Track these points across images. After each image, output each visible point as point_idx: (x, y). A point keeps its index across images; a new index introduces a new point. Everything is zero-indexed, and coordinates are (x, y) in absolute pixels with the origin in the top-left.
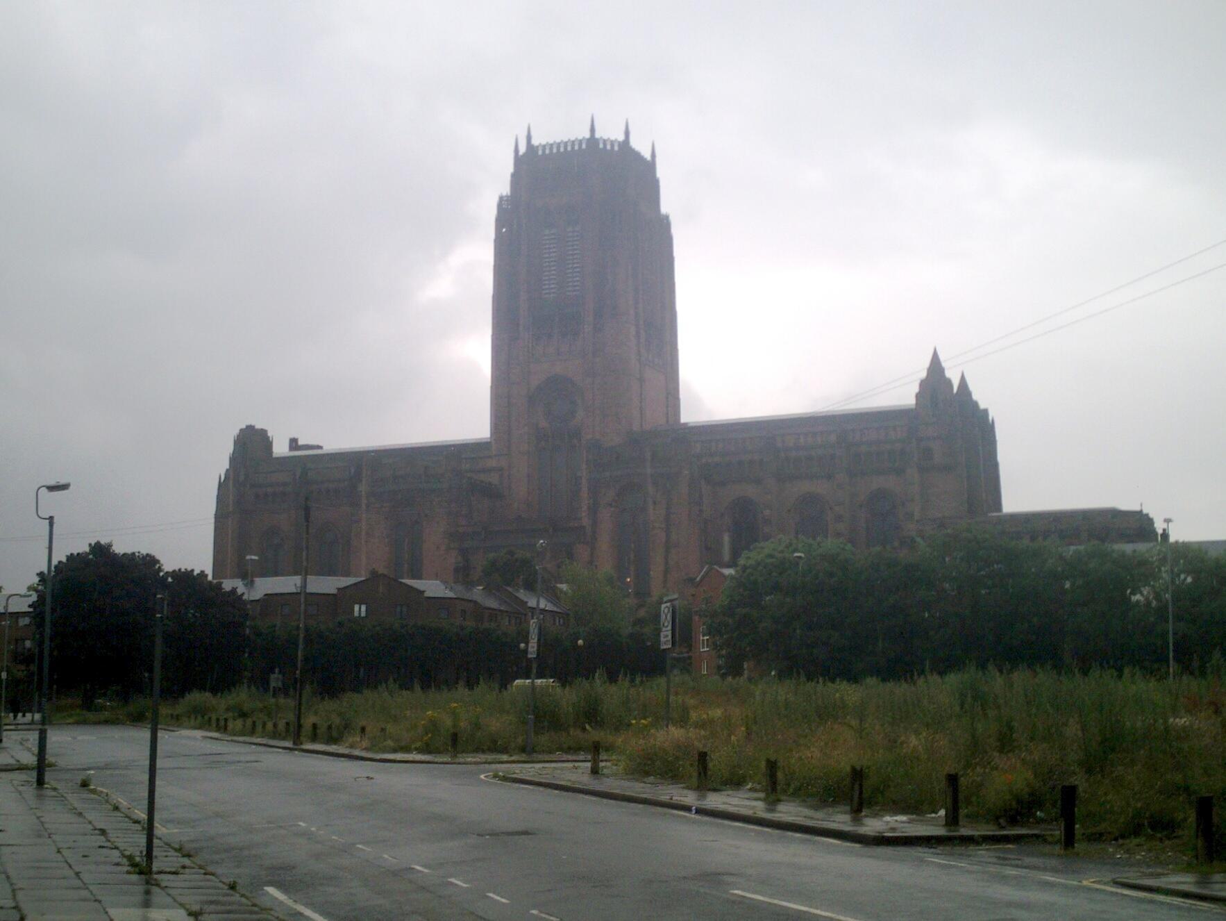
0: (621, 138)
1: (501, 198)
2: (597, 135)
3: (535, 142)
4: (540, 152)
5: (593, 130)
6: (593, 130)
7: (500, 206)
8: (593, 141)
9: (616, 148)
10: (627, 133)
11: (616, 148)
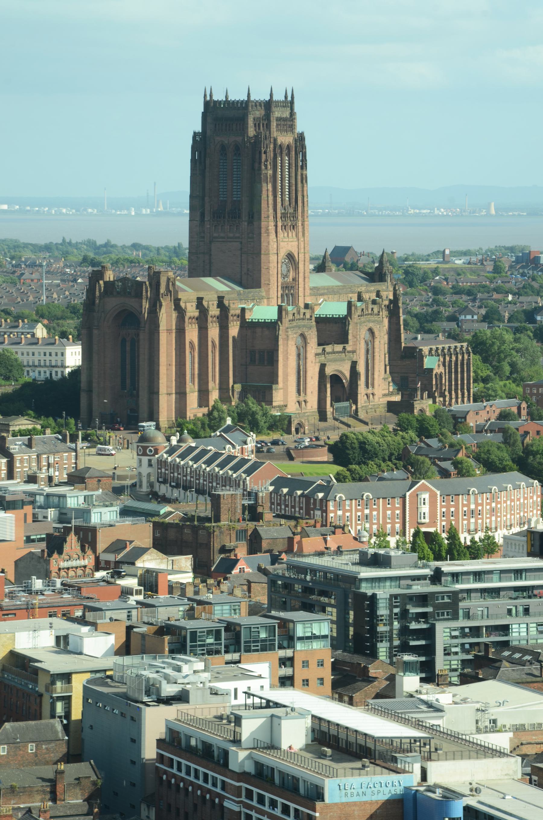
10: (271, 95)
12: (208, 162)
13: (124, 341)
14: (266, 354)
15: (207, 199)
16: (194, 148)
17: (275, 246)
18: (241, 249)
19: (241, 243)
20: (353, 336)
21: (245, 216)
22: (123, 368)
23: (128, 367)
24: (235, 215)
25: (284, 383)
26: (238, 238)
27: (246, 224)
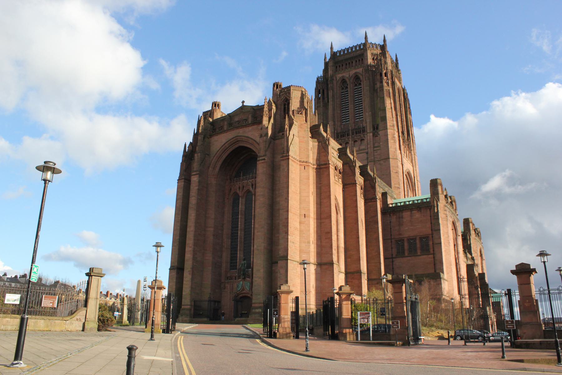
0: (382, 43)
1: (317, 79)
4: (338, 54)
5: (366, 38)
6: (366, 38)
7: (318, 82)
10: (385, 41)
12: (330, 94)
14: (418, 241)
18: (368, 158)
19: (367, 153)
21: (369, 129)
22: (234, 236)
23: (240, 234)
24: (360, 131)
26: (364, 149)
27: (371, 134)
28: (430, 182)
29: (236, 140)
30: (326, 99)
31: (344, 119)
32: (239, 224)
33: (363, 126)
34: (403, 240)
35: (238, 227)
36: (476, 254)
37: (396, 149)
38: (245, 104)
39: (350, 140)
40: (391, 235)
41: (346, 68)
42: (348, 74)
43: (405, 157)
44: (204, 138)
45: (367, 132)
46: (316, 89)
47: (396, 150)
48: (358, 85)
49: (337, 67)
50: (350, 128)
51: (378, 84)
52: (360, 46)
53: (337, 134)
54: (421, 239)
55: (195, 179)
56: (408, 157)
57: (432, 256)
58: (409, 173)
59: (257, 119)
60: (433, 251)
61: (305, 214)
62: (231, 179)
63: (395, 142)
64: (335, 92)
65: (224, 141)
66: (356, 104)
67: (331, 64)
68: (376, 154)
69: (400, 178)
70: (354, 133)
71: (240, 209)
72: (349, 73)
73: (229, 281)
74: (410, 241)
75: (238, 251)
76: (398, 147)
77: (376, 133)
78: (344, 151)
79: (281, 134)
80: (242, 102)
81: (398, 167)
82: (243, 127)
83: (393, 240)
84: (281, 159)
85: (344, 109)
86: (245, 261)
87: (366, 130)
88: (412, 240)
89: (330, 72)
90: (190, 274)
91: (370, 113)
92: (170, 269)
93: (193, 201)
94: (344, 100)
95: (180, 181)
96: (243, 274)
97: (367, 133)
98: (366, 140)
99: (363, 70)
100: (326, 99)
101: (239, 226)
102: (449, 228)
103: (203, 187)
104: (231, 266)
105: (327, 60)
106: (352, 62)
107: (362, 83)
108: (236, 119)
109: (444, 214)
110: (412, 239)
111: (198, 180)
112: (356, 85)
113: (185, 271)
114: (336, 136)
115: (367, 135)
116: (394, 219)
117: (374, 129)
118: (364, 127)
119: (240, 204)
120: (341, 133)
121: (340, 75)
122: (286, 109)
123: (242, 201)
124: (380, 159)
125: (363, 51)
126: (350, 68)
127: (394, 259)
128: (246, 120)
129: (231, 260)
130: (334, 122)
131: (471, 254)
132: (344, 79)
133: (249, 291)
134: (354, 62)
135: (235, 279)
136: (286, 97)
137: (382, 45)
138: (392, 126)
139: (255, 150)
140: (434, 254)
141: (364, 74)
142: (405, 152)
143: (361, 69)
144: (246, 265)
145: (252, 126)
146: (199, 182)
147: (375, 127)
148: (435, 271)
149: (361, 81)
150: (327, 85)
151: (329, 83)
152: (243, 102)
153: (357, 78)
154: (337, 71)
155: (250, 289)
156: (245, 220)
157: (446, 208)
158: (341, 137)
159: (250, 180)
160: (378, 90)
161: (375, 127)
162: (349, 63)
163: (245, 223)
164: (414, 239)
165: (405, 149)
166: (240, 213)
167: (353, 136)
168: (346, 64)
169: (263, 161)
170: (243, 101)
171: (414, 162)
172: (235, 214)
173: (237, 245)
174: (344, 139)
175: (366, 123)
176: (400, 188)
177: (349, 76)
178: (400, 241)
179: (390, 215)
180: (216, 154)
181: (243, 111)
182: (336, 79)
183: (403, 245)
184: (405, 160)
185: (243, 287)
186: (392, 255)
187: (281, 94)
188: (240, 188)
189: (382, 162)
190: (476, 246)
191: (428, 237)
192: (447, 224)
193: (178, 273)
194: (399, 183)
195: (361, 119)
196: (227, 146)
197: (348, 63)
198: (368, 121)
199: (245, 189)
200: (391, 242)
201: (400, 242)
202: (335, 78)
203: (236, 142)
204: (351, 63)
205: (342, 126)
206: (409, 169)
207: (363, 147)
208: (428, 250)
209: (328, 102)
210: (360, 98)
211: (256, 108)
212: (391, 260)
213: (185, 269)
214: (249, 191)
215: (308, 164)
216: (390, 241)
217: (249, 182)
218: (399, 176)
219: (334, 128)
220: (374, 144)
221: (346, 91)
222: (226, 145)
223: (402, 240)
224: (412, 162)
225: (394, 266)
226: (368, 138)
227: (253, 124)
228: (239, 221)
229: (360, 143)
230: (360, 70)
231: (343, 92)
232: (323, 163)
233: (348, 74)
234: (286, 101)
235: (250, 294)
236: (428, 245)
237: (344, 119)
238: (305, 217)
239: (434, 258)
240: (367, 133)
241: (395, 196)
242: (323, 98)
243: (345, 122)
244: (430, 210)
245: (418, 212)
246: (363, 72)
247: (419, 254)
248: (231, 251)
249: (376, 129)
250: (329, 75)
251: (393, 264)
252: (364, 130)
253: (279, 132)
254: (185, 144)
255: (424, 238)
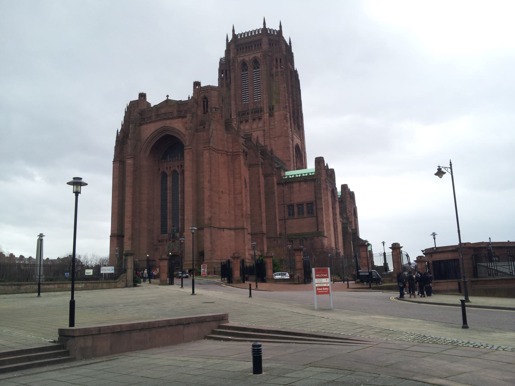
0: (278, 29)
1: (221, 60)
2: (267, 27)
3: (236, 33)
4: (239, 37)
5: (264, 24)
6: (264, 24)
7: (220, 63)
8: (265, 29)
9: (276, 33)
10: (281, 27)
11: (276, 33)
12: (232, 75)
13: (164, 176)
15: (233, 102)
16: (221, 71)
17: (291, 134)
18: (264, 135)
19: (264, 131)
20: (349, 211)
21: (266, 110)
25: (327, 232)
27: (268, 114)
28: (315, 159)
29: (164, 129)
30: (228, 80)
31: (245, 99)
32: (168, 197)
33: (260, 107)
34: (293, 205)
35: (167, 200)
36: (350, 213)
37: (287, 127)
38: (169, 98)
39: (250, 118)
40: (284, 201)
41: (247, 52)
42: (248, 57)
43: (295, 134)
44: (135, 126)
45: (264, 112)
46: (219, 70)
47: (288, 129)
48: (256, 68)
49: (238, 50)
50: (250, 108)
51: (274, 69)
52: (259, 30)
53: (239, 112)
54: (307, 204)
55: (130, 162)
56: (297, 133)
57: (315, 218)
58: (297, 147)
59: (181, 113)
60: (317, 214)
61: (222, 192)
62: (159, 160)
63: (287, 122)
64: (237, 74)
65: (153, 130)
66: (254, 86)
67: (232, 46)
68: (271, 131)
69: (291, 152)
70: (253, 112)
71: (168, 186)
72: (249, 57)
73: (161, 243)
74: (299, 206)
75: (168, 219)
76: (290, 126)
77: (272, 114)
78: (250, 138)
79: (202, 127)
80: (167, 96)
81: (289, 143)
82: (169, 119)
83: (285, 205)
84: (204, 149)
85: (244, 90)
86: (175, 227)
87: (263, 111)
88: (300, 205)
89: (232, 55)
90: (129, 240)
91: (267, 95)
92: (110, 236)
93: (129, 180)
94: (244, 82)
95: (115, 162)
96: (173, 238)
97: (264, 113)
98: (263, 119)
99: (261, 54)
100: (228, 80)
101: (168, 199)
102: (329, 196)
103: (137, 169)
104: (162, 231)
105: (229, 41)
106: (252, 47)
107: (260, 66)
108: (163, 111)
109: (325, 185)
110: (300, 205)
111: (132, 163)
112: (255, 68)
113: (125, 237)
114: (237, 115)
115: (264, 115)
116: (286, 188)
117: (270, 109)
118: (261, 107)
119: (168, 182)
120: (241, 112)
121: (241, 58)
122: (206, 106)
123: (169, 179)
124: (275, 136)
125: (261, 36)
126: (250, 52)
127: (286, 221)
128: (172, 113)
129: (162, 226)
130: (236, 101)
131: (346, 214)
132: (244, 62)
133: (179, 251)
134: (253, 47)
135: (167, 242)
136: (205, 96)
137: (278, 30)
138: (285, 108)
139: (179, 138)
140: (317, 217)
141: (262, 59)
142: (295, 128)
143: (260, 53)
144: (175, 230)
145: (177, 118)
146: (134, 164)
147: (271, 108)
148: (318, 230)
149: (259, 65)
150: (230, 66)
151: (231, 65)
152: (168, 96)
153: (256, 62)
154: (238, 54)
155: (179, 249)
156: (173, 194)
157: (326, 180)
158: (242, 115)
159: (176, 162)
160: (274, 74)
161: (271, 108)
162: (249, 47)
163: (172, 197)
164: (302, 205)
165: (295, 126)
166: (168, 188)
167: (252, 115)
168: (246, 48)
169: (189, 150)
170: (167, 95)
171: (302, 136)
172: (164, 190)
173: (167, 214)
174: (244, 118)
175: (263, 104)
176: (290, 161)
177: (249, 59)
178: (291, 206)
179: (283, 186)
180: (147, 140)
181: (168, 104)
182: (238, 62)
183: (293, 209)
184: (295, 137)
185: (173, 248)
186: (285, 217)
187: (201, 92)
188: (167, 168)
189: (276, 139)
190: (350, 207)
191: (313, 203)
192: (328, 193)
193: (118, 239)
194: (290, 157)
195: (258, 100)
196: (156, 134)
197: (248, 47)
198: (265, 102)
199: (172, 169)
200: (284, 207)
201: (291, 207)
202: (236, 60)
203: (163, 131)
204: (250, 47)
205: (243, 105)
206: (298, 143)
207: (261, 124)
208: (312, 213)
209: (230, 82)
210: (258, 81)
211: (179, 103)
212: (284, 221)
213: (125, 236)
214: (175, 171)
215: (224, 152)
216: (283, 206)
217: (175, 164)
218: (290, 151)
219: (236, 107)
220: (270, 123)
221: (246, 74)
222: (155, 133)
223: (292, 205)
224: (300, 137)
225: (286, 226)
226: (265, 117)
227: (179, 117)
228: (168, 195)
229: (258, 121)
230: (258, 55)
231: (244, 74)
232: (235, 151)
233: (248, 57)
234: (205, 99)
235: (179, 253)
236: (312, 210)
237: (245, 99)
238: (222, 193)
239: (317, 219)
240: (264, 113)
241: (287, 168)
242: (226, 79)
243: (245, 101)
244: (314, 182)
245: (305, 183)
246: (261, 57)
247: (305, 216)
248: (161, 219)
249: (271, 110)
250: (231, 57)
251: (285, 224)
252: (261, 110)
253: (200, 125)
254: (117, 130)
255: (310, 204)
